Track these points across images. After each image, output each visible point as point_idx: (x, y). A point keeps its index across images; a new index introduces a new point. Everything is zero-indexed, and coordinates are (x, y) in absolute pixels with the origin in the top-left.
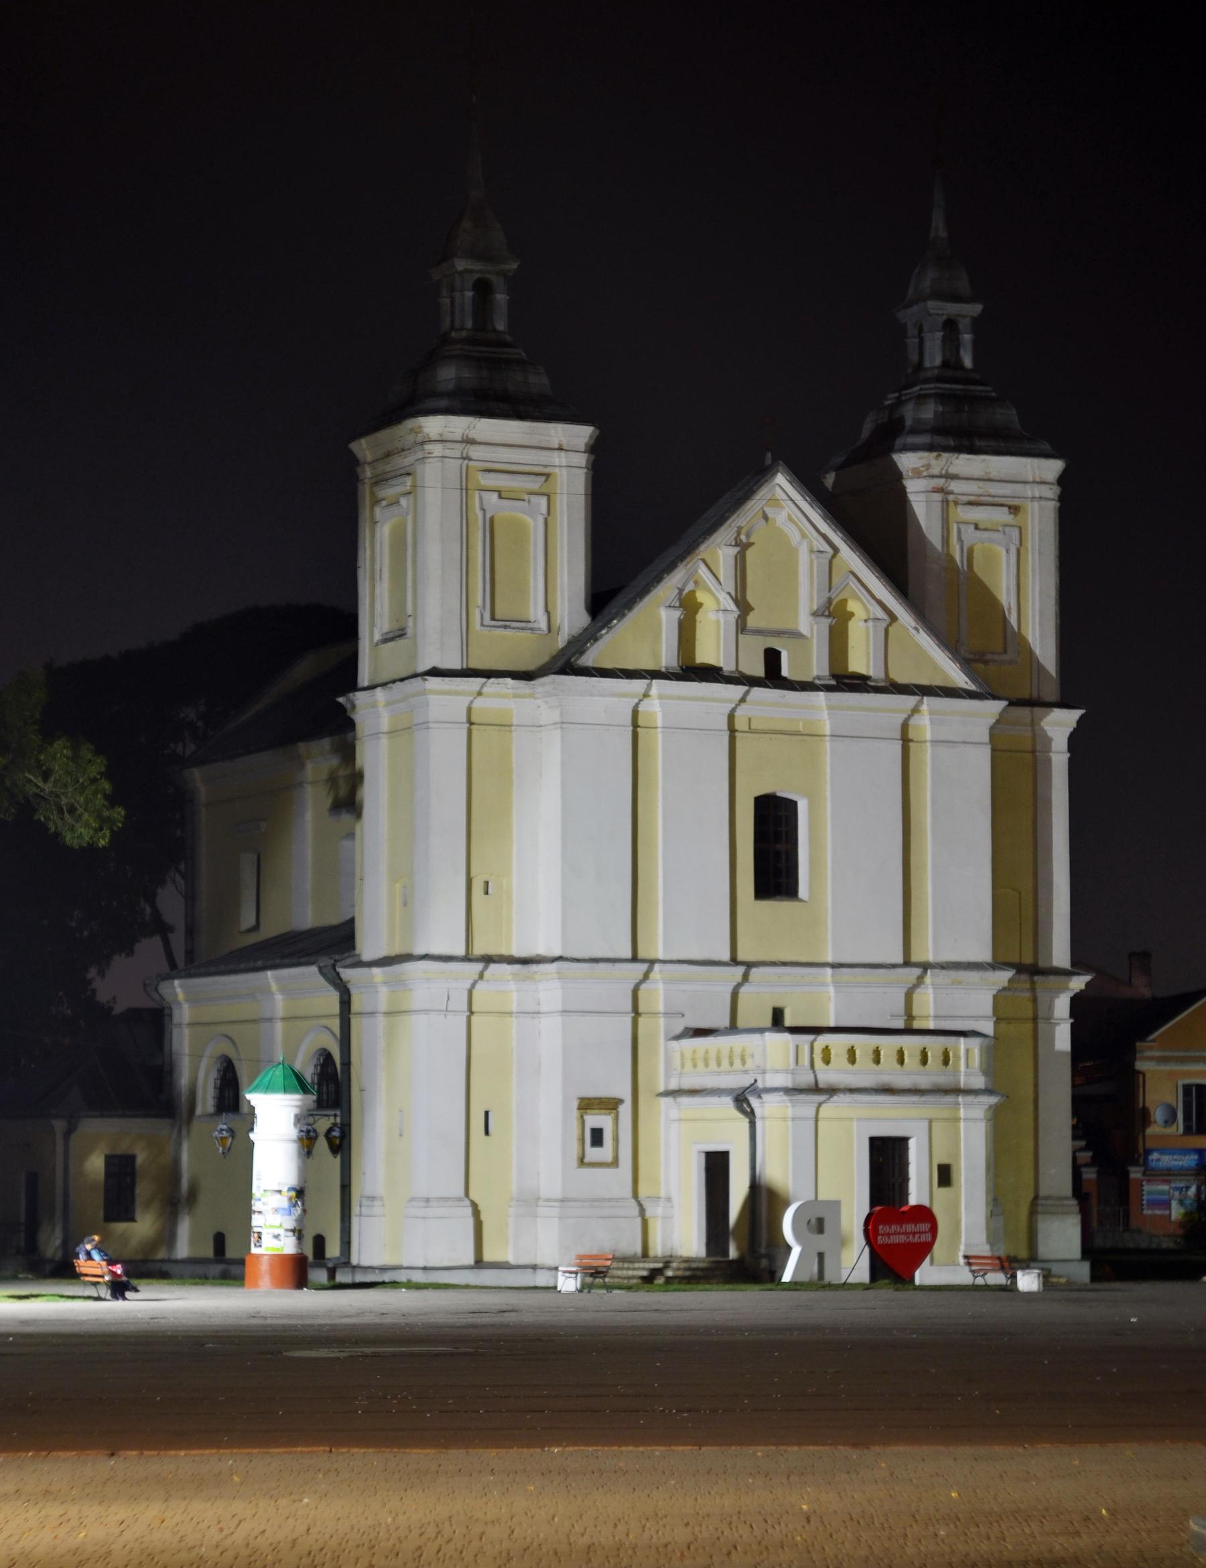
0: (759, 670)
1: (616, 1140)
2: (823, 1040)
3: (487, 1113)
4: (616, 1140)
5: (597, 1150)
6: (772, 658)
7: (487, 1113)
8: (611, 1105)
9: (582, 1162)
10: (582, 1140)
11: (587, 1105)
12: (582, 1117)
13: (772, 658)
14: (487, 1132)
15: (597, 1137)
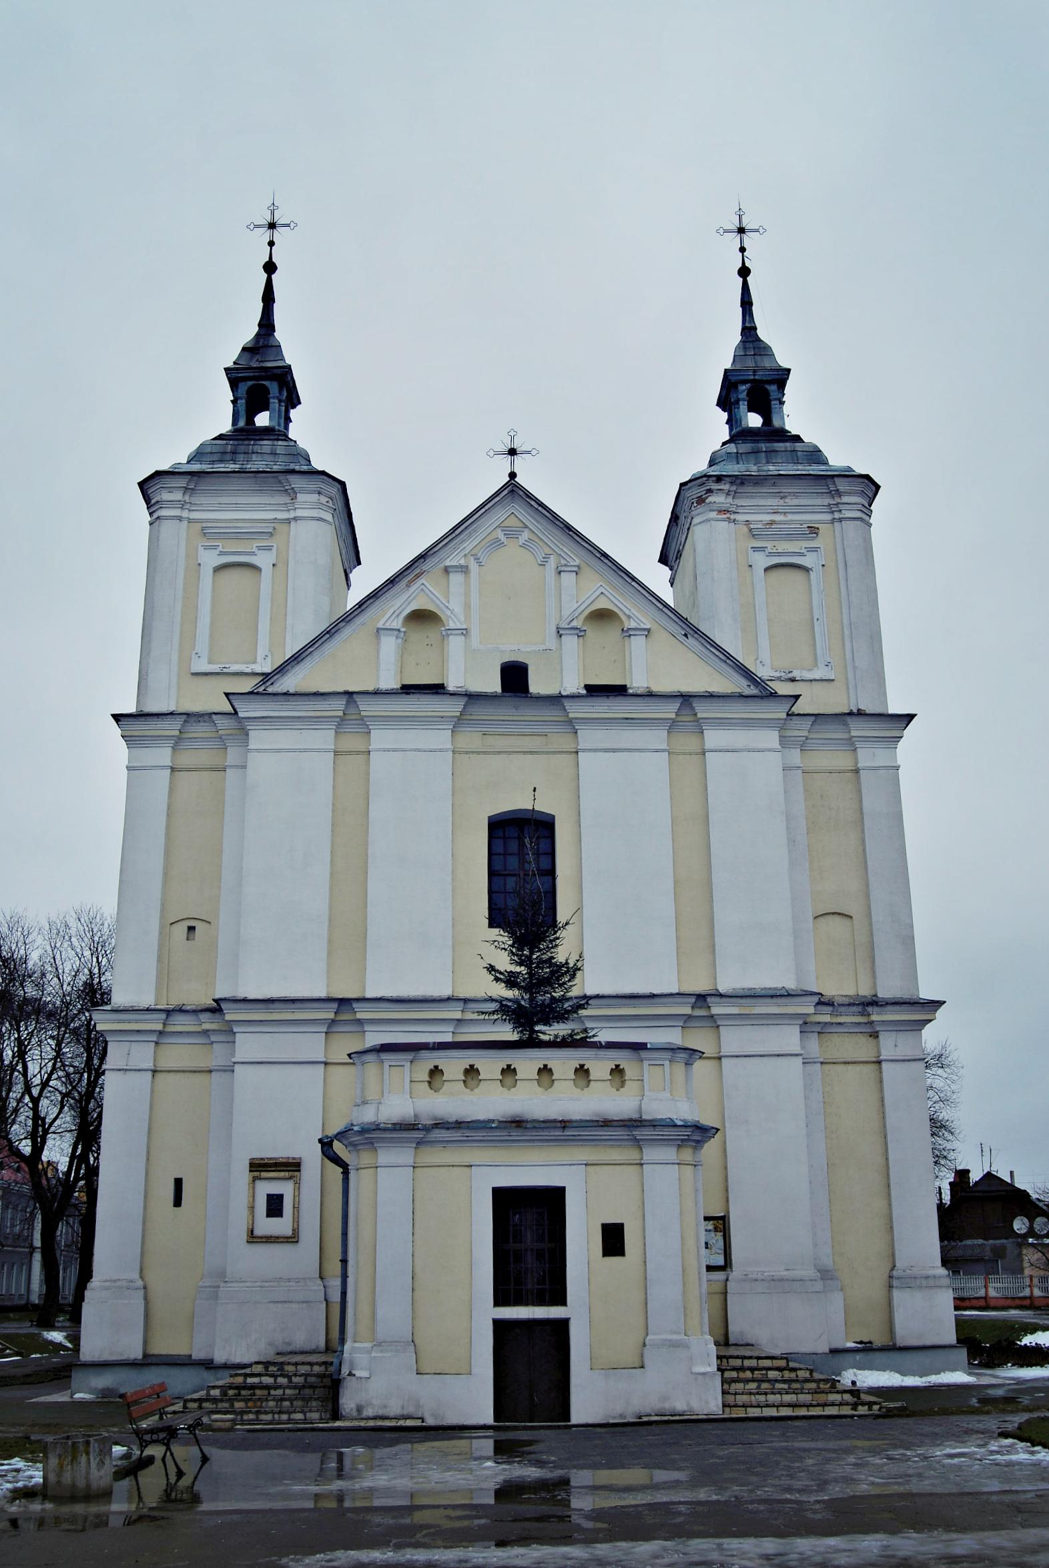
0: (494, 684)
1: (296, 1208)
2: (428, 1061)
3: (178, 1183)
4: (296, 1208)
5: (274, 1220)
6: (515, 677)
7: (178, 1183)
8: (291, 1167)
9: (253, 1238)
10: (252, 1208)
11: (259, 1167)
12: (254, 1179)
13: (515, 677)
14: (178, 1202)
15: (275, 1206)
